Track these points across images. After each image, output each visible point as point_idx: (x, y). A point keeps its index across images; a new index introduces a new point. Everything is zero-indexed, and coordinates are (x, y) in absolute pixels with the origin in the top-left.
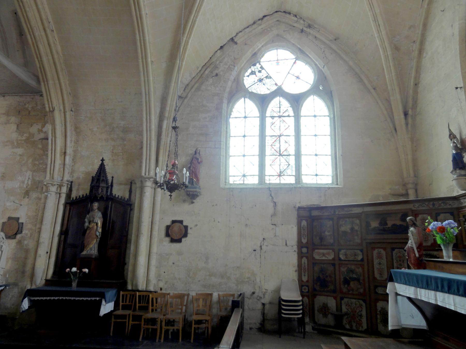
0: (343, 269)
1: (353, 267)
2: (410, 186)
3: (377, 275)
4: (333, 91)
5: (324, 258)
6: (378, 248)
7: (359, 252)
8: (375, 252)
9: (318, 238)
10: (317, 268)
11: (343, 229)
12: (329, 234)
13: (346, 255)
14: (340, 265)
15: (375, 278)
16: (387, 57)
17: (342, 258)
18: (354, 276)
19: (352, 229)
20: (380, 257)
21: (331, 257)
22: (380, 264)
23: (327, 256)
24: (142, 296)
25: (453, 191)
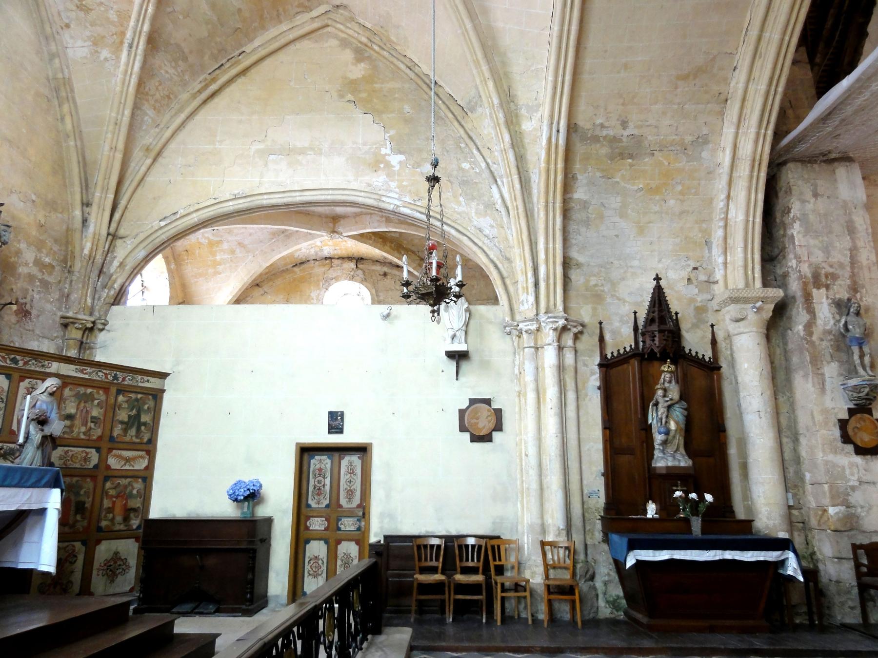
24: (496, 546)
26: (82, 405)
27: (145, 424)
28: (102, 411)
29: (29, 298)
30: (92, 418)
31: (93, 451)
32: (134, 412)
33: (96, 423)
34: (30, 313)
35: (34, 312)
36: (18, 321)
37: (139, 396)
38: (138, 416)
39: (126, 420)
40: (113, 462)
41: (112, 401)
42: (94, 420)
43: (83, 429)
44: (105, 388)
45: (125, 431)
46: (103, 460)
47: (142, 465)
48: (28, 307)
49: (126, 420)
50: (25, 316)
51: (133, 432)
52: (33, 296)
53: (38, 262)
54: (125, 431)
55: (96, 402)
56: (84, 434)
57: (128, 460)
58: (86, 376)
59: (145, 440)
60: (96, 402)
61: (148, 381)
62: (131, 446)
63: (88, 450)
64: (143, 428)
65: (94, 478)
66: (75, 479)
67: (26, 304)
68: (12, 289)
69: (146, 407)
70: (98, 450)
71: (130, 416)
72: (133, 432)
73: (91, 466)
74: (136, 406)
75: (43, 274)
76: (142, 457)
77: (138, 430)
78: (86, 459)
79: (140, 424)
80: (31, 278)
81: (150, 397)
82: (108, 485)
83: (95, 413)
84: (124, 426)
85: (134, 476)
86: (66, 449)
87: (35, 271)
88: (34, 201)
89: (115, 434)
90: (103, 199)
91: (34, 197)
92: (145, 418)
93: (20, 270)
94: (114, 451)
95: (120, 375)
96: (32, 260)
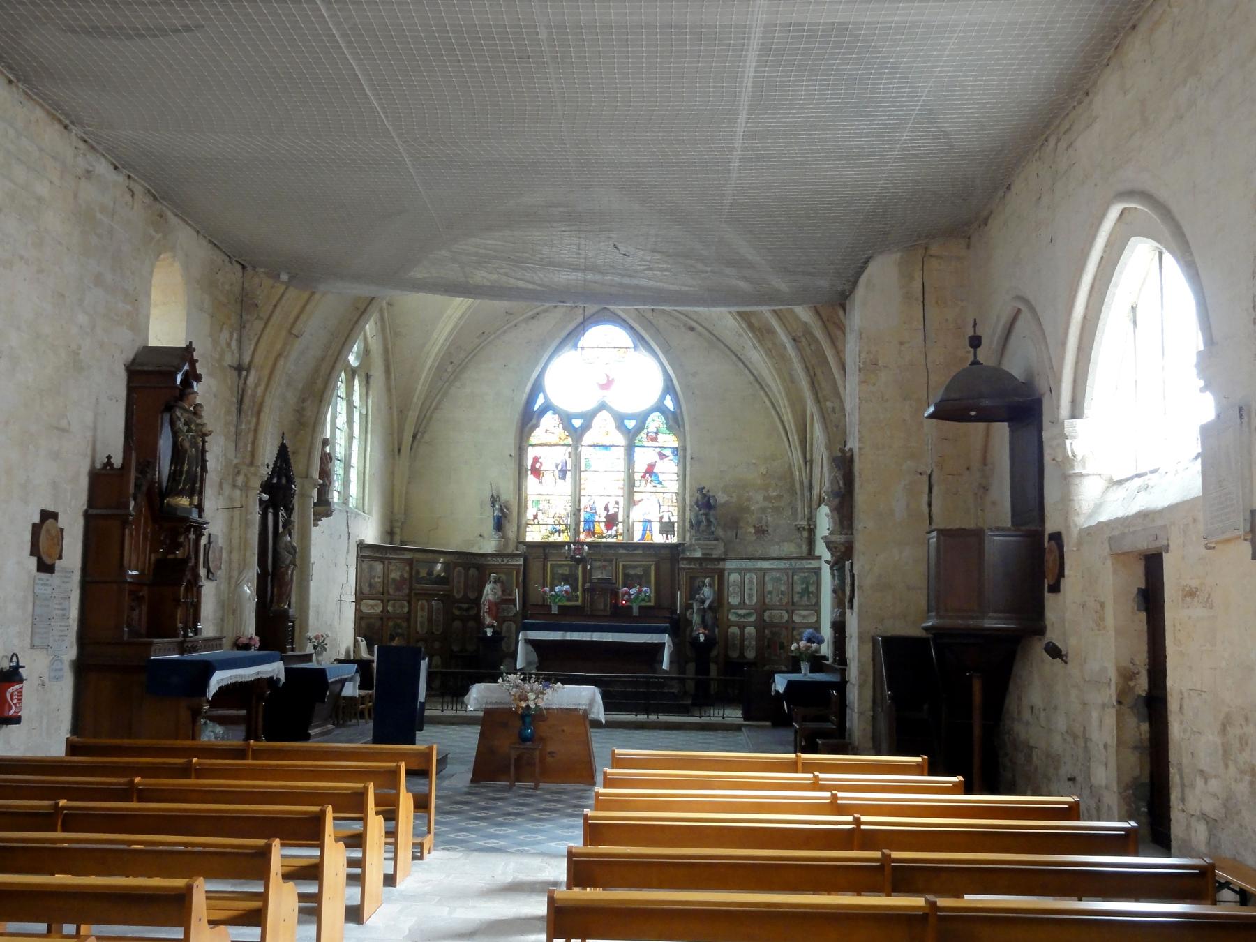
0: (390, 624)
1: (399, 621)
2: (399, 524)
3: (419, 629)
4: (372, 377)
5: (372, 611)
6: (422, 599)
7: (406, 603)
8: (420, 603)
9: (367, 585)
10: (363, 624)
11: (393, 575)
12: (379, 580)
13: (394, 606)
14: (389, 619)
15: (417, 632)
16: (431, 368)
17: (390, 611)
18: (400, 631)
19: (402, 576)
20: (423, 609)
21: (379, 609)
22: (422, 617)
23: (375, 608)
25: (473, 546)
26: (775, 584)
27: (812, 592)
28: (786, 587)
29: (764, 522)
30: (782, 592)
31: (784, 612)
32: (804, 586)
33: (783, 595)
34: (767, 531)
35: (770, 530)
36: (757, 538)
37: (806, 574)
38: (807, 588)
39: (800, 591)
40: (797, 619)
41: (790, 580)
42: (783, 593)
43: (778, 599)
44: (785, 571)
45: (801, 597)
46: (791, 617)
47: (813, 620)
48: (764, 527)
49: (800, 591)
50: (763, 534)
51: (805, 598)
52: (767, 520)
53: (765, 499)
54: (801, 597)
55: (782, 582)
56: (779, 601)
57: (804, 617)
58: (775, 567)
59: (813, 603)
60: (782, 582)
61: (810, 563)
62: (806, 607)
63: (781, 611)
64: (811, 595)
65: (787, 628)
66: (777, 629)
67: (762, 526)
68: (748, 522)
69: (811, 581)
70: (787, 611)
71: (802, 589)
72: (805, 598)
73: (784, 621)
74: (805, 581)
75: (773, 503)
76: (813, 615)
77: (809, 597)
78: (781, 617)
79: (809, 593)
80: (763, 510)
81: (813, 574)
82: (795, 633)
83: (783, 588)
84: (799, 595)
85: (808, 626)
86: (770, 611)
87: (766, 504)
88: (754, 464)
89: (795, 601)
90: (795, 438)
91: (754, 461)
92: (812, 589)
93: (752, 508)
94: (797, 612)
95: (793, 562)
96: (762, 498)
